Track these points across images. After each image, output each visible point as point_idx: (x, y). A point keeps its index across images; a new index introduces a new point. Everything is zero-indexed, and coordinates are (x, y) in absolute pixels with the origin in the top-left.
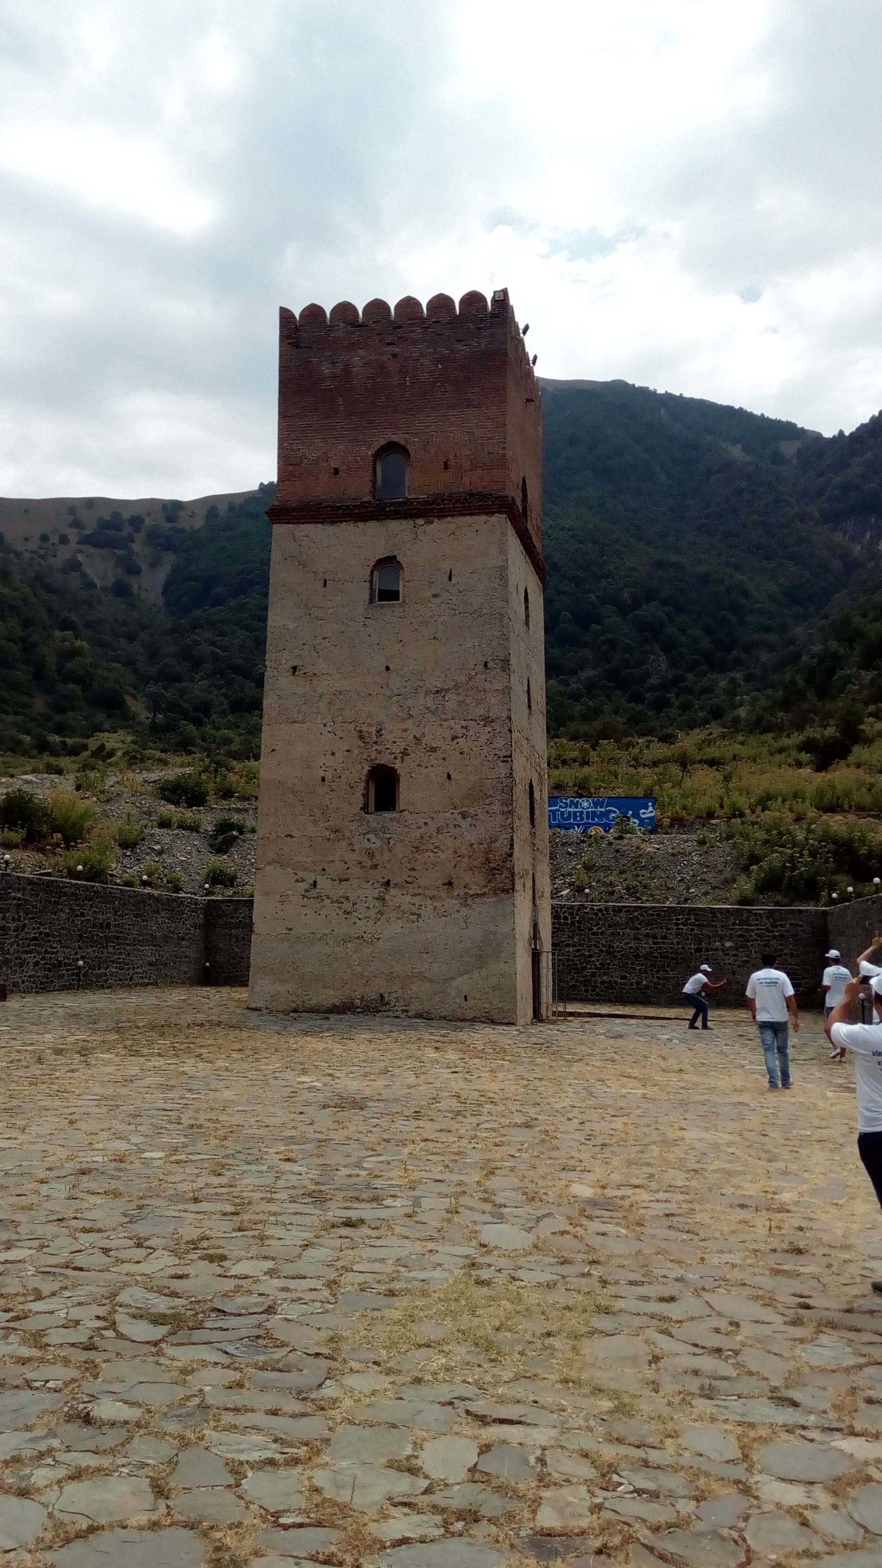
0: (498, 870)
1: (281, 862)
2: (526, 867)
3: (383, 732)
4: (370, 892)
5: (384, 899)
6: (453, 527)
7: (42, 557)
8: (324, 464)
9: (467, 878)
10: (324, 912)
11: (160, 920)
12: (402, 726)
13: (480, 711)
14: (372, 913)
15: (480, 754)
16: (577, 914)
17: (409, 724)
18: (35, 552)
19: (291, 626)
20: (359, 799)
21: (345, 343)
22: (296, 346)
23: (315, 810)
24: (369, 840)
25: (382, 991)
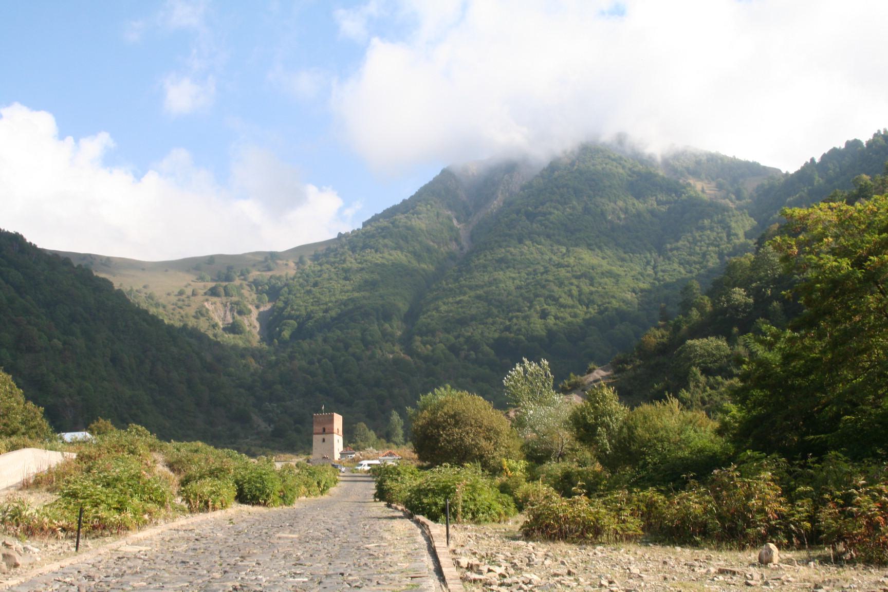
7: (181, 308)
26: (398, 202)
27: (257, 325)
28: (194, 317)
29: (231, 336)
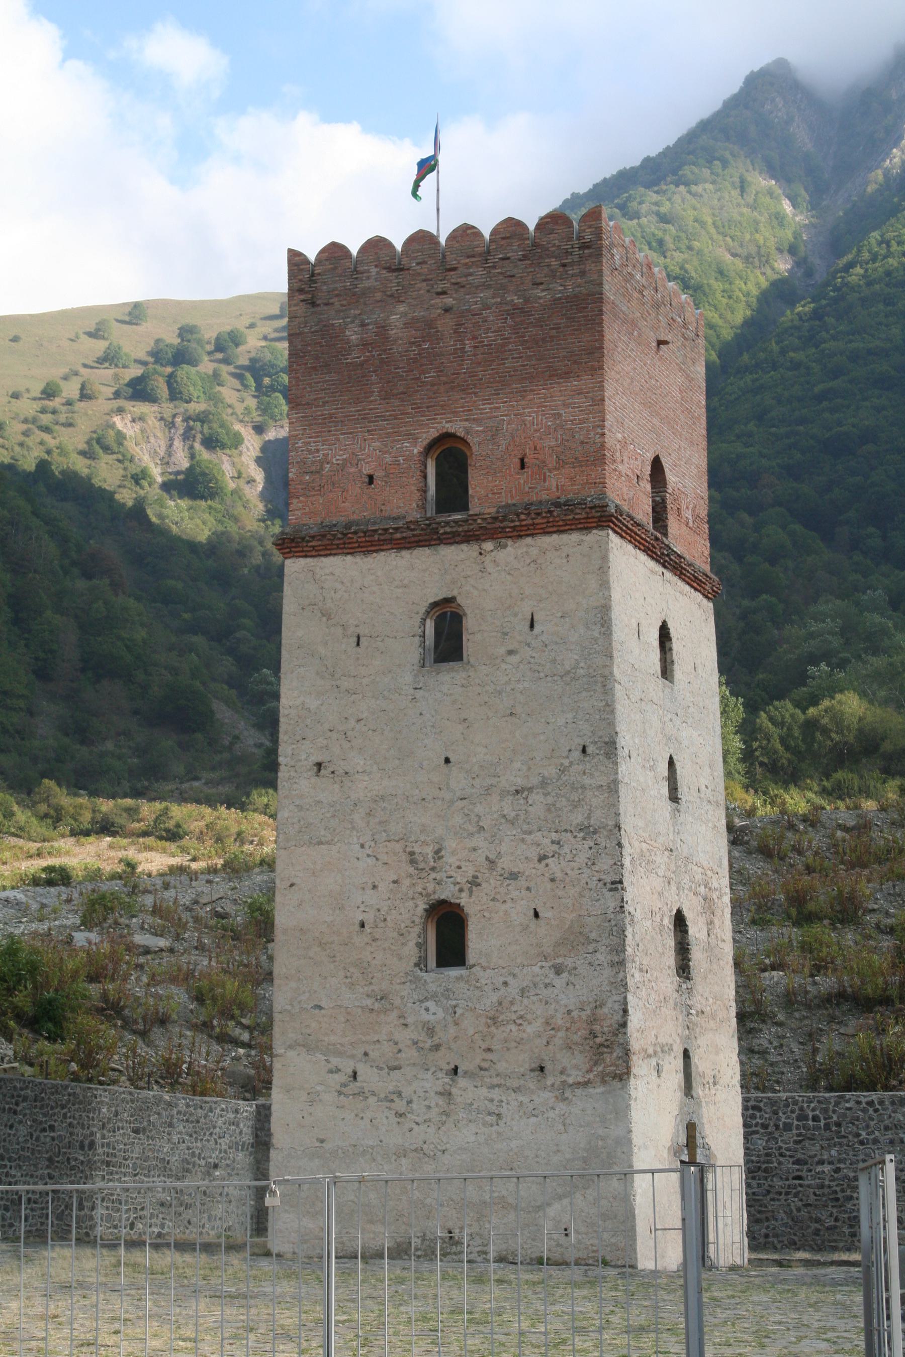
0: (608, 1047)
1: (308, 1046)
2: (662, 1040)
3: (443, 853)
4: (431, 1083)
5: (450, 1094)
6: (534, 552)
7: (47, 429)
8: (352, 470)
9: (565, 1059)
10: (368, 1115)
11: (175, 1138)
13: (578, 818)
14: (434, 1114)
15: (579, 880)
16: (834, 1111)
17: (479, 841)
18: (34, 421)
19: (313, 703)
20: (410, 950)
21: (378, 296)
22: (313, 304)
23: (352, 970)
24: (427, 1010)
25: (450, 1225)
26: (635, 161)
27: (259, 476)
28: (83, 453)
29: (184, 503)
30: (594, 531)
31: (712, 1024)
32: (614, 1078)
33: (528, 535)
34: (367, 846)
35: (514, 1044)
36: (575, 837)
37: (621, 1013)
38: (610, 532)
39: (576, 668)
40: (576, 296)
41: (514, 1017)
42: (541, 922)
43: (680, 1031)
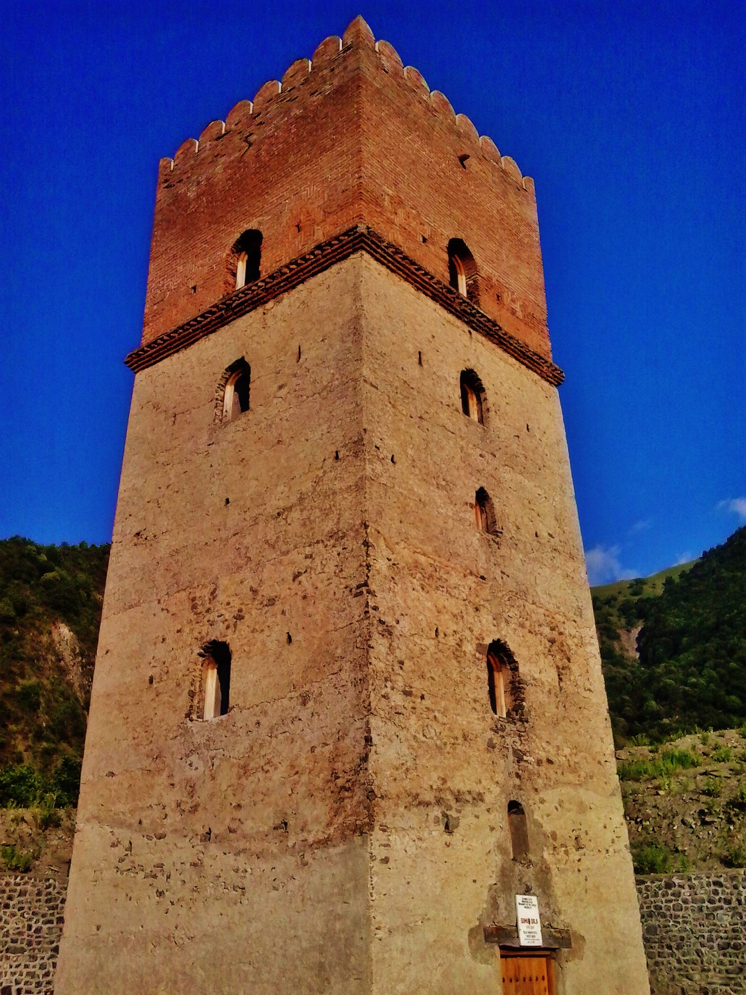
0: (348, 790)
12: (238, 577)
13: (329, 526)
17: (246, 573)
21: (210, 159)
24: (191, 765)
30: (352, 256)
31: (571, 777)
32: (354, 831)
33: (298, 284)
34: (162, 602)
35: (261, 797)
36: (326, 546)
37: (363, 742)
38: (364, 252)
39: (332, 381)
40: (341, 86)
41: (262, 763)
42: (293, 647)
43: (500, 777)
